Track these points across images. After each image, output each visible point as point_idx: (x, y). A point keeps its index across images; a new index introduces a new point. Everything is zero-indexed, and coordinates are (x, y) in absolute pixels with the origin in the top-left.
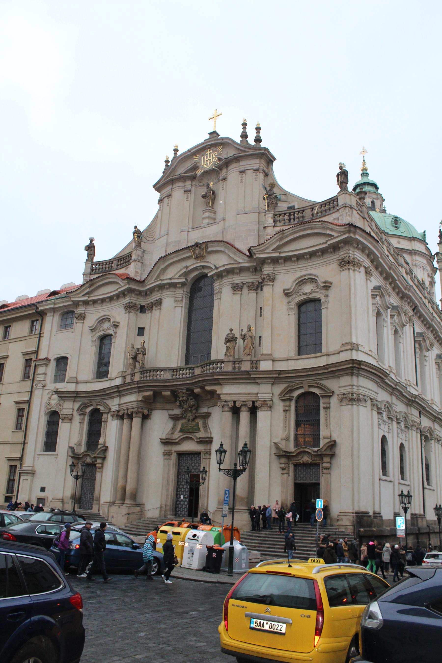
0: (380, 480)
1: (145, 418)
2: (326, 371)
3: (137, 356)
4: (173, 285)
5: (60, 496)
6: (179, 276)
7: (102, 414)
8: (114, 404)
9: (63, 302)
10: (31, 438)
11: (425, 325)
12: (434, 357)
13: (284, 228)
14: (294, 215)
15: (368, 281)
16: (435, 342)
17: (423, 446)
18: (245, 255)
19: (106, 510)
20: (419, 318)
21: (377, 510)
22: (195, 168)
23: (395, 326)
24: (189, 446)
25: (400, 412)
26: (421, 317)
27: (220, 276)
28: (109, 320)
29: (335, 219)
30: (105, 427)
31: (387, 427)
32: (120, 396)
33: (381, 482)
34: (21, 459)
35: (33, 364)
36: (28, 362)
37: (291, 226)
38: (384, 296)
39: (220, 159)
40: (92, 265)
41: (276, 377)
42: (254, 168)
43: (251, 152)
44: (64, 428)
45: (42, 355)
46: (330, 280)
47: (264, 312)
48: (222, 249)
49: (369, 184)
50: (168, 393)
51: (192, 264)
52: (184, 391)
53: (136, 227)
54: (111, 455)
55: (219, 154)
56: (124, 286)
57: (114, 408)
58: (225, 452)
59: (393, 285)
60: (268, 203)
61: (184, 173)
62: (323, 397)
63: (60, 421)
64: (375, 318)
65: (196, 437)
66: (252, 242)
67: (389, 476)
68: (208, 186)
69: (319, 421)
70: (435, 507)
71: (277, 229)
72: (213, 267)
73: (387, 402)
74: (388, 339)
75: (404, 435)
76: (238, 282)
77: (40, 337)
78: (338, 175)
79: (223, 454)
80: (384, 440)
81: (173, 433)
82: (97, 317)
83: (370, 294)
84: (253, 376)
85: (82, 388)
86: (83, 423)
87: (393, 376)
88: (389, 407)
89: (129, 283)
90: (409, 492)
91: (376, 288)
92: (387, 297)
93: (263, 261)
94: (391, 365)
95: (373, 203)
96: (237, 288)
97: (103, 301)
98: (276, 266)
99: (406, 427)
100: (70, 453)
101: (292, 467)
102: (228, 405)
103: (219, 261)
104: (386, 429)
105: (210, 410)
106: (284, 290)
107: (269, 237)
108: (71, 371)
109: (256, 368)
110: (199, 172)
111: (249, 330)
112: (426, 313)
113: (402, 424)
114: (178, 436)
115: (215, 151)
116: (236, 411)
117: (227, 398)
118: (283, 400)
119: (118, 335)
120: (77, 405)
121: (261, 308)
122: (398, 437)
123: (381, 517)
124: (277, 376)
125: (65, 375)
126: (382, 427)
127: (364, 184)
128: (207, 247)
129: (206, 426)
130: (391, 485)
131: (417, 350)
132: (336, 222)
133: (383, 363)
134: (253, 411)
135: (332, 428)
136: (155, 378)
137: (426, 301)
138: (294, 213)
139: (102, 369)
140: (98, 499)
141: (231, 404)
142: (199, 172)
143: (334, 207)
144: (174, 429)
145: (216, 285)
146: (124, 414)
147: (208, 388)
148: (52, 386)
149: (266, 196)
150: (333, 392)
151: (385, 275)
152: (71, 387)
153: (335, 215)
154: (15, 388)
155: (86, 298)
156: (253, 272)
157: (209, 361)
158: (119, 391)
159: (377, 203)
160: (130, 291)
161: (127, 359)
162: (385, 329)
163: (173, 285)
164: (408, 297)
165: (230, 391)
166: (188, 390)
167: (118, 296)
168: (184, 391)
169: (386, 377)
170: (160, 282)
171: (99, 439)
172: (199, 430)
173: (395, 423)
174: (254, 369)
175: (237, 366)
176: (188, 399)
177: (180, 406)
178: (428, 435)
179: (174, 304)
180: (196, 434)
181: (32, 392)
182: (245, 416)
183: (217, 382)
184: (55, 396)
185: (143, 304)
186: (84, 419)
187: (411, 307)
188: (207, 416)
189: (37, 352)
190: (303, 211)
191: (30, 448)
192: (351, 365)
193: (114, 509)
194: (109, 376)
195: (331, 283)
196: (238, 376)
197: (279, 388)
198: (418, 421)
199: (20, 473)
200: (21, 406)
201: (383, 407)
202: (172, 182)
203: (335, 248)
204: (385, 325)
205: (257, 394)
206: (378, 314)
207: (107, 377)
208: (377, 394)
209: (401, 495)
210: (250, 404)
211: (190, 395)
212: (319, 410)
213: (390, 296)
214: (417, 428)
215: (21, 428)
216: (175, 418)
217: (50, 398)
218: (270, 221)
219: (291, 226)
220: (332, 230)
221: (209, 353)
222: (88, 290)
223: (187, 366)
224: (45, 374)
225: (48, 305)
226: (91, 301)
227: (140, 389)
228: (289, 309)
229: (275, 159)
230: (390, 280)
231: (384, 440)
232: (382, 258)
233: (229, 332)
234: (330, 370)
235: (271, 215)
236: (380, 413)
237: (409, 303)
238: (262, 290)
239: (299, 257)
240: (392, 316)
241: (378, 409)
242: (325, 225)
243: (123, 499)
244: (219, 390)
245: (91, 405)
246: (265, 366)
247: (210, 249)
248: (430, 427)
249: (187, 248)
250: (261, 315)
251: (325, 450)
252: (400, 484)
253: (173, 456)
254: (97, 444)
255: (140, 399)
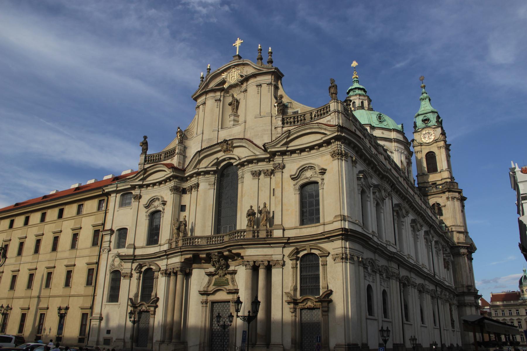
0: (367, 319)
1: (187, 275)
2: (323, 237)
3: (180, 227)
4: (207, 173)
5: (122, 337)
6: (213, 165)
7: (154, 272)
8: (162, 264)
9: (123, 186)
10: (99, 291)
11: (401, 198)
12: (409, 222)
13: (290, 128)
14: (297, 118)
15: (354, 168)
16: (410, 210)
17: (402, 291)
18: (261, 149)
19: (158, 347)
20: (397, 192)
21: (365, 341)
22: (224, 82)
23: (376, 200)
24: (221, 296)
25: (382, 266)
26: (397, 192)
27: (242, 165)
28: (158, 199)
29: (328, 121)
30: (157, 282)
31: (371, 278)
32: (168, 259)
33: (368, 321)
34: (92, 308)
35: (101, 234)
36: (96, 233)
37: (295, 127)
38: (367, 178)
39: (242, 76)
40: (146, 157)
41: (287, 242)
42: (267, 83)
43: (265, 70)
44: (124, 283)
45: (108, 227)
46: (325, 168)
47: (276, 192)
48: (244, 145)
49: (359, 89)
50: (204, 256)
51: (221, 155)
52: (216, 254)
53: (179, 128)
54: (161, 304)
55: (241, 72)
56: (169, 173)
57: (163, 268)
58: (241, 303)
59: (374, 169)
60: (278, 109)
61: (215, 86)
62: (321, 257)
63: (122, 278)
64: (360, 195)
65: (226, 289)
66: (267, 140)
67: (374, 316)
68: (233, 96)
69: (319, 275)
70: (410, 338)
71: (285, 129)
72: (238, 159)
73: (371, 259)
74: (371, 210)
75: (386, 283)
76: (256, 169)
77: (106, 213)
78: (330, 88)
79: (240, 305)
80: (369, 288)
81: (208, 287)
82: (150, 198)
83: (355, 176)
84: (268, 241)
85: (138, 252)
86: (140, 279)
87: (375, 239)
88: (372, 263)
89: (173, 172)
90: (387, 328)
91: (360, 172)
92: (369, 179)
93: (273, 154)
94: (374, 230)
95: (362, 103)
96: (256, 174)
97: (154, 184)
98: (284, 157)
99: (387, 277)
100: (130, 303)
101: (298, 311)
102: (249, 264)
103: (241, 153)
104: (371, 280)
105: (236, 268)
106: (291, 176)
107: (279, 135)
108: (129, 240)
109: (271, 235)
110: (226, 86)
111: (265, 207)
112: (402, 189)
113: (384, 275)
114: (212, 289)
115: (238, 70)
116: (255, 269)
117: (249, 259)
118: (291, 260)
119: (165, 211)
120: (135, 265)
121: (274, 189)
122: (381, 285)
123: (368, 347)
124: (286, 241)
125: (125, 242)
126: (367, 278)
127: (356, 88)
128: (232, 143)
129: (233, 280)
130: (375, 323)
131: (395, 217)
132: (329, 123)
133: (367, 229)
134: (269, 269)
135: (328, 281)
136: (194, 244)
137: (401, 180)
138: (298, 116)
139: (153, 236)
140: (152, 339)
141: (252, 263)
142: (226, 86)
143: (327, 112)
144: (209, 282)
145: (240, 172)
146: (170, 272)
147: (234, 251)
148: (114, 251)
149: (276, 104)
150: (329, 253)
151: (367, 162)
152: (130, 252)
153: (329, 118)
154: (87, 252)
155: (141, 183)
156: (267, 162)
157: (235, 231)
158: (167, 255)
159: (366, 103)
160: (174, 177)
161: (173, 230)
162: (369, 203)
163: (207, 173)
164: (387, 177)
165: (252, 253)
166: (219, 253)
167: (165, 181)
168: (216, 254)
169: (369, 240)
170: (197, 170)
171: (152, 291)
172: (228, 284)
173: (378, 275)
174: (269, 237)
175: (256, 234)
176: (219, 260)
177: (214, 265)
178: (406, 282)
179: (209, 187)
180: (225, 287)
181: (99, 255)
182: (262, 273)
183: (241, 246)
184: (118, 259)
185: (185, 187)
186: (140, 276)
187: (389, 184)
188: (234, 272)
189: (103, 224)
190: (304, 115)
191: (98, 299)
192: (341, 232)
193: (164, 346)
194: (159, 243)
195: (326, 170)
196: (257, 242)
197: (288, 250)
198: (397, 271)
199: (91, 320)
200: (91, 267)
201: (368, 263)
202: (206, 93)
203: (328, 143)
204: (369, 200)
205: (272, 255)
206: (363, 192)
207: (158, 244)
208: (363, 253)
209: (382, 331)
210: (266, 263)
211: (220, 257)
212: (318, 266)
213: (372, 178)
214: (397, 278)
215: (91, 284)
216: (210, 275)
217: (113, 261)
218: (280, 123)
219: (295, 127)
220: (325, 129)
221: (235, 225)
222: (142, 177)
223: (218, 235)
224: (110, 242)
225: (112, 188)
226: (145, 185)
227: (182, 253)
228: (295, 190)
229: (283, 76)
230: (372, 165)
231: (369, 288)
232: (364, 149)
233: (249, 208)
234: (326, 236)
235: (280, 119)
236: (365, 268)
237: (387, 182)
238: (274, 176)
239: (302, 150)
240: (374, 193)
241: (364, 264)
242: (320, 126)
243: (171, 338)
244: (242, 252)
245: (146, 265)
246: (277, 233)
247: (234, 145)
248: (407, 277)
249: (218, 144)
250: (274, 195)
251: (324, 298)
252: (383, 321)
253: (208, 304)
254: (150, 296)
255: (183, 261)
